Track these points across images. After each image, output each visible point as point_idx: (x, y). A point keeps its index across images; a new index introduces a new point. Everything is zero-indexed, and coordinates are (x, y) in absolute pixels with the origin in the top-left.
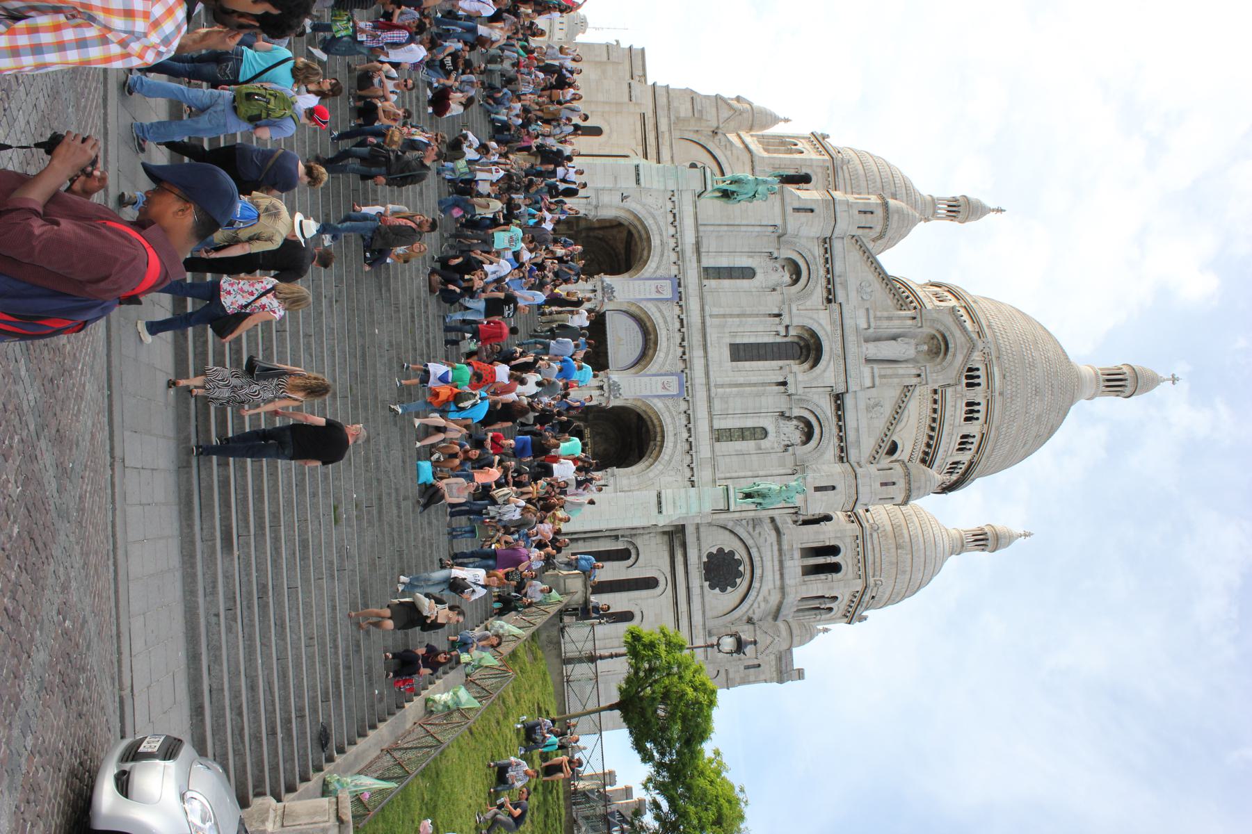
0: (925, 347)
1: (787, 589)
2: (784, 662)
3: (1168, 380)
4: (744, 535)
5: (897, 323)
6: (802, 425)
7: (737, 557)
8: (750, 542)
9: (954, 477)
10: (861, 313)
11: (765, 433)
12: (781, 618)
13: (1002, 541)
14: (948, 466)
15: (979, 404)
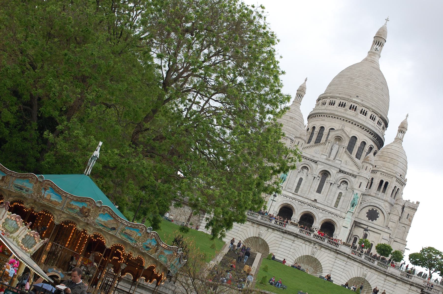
0: (338, 142)
1: (386, 199)
2: (411, 206)
3: (386, 22)
4: (366, 205)
5: (328, 148)
6: (343, 183)
7: (371, 209)
8: (368, 204)
9: (383, 124)
10: (322, 156)
11: (341, 193)
12: (393, 204)
13: (405, 126)
14: (378, 125)
15: (362, 109)
